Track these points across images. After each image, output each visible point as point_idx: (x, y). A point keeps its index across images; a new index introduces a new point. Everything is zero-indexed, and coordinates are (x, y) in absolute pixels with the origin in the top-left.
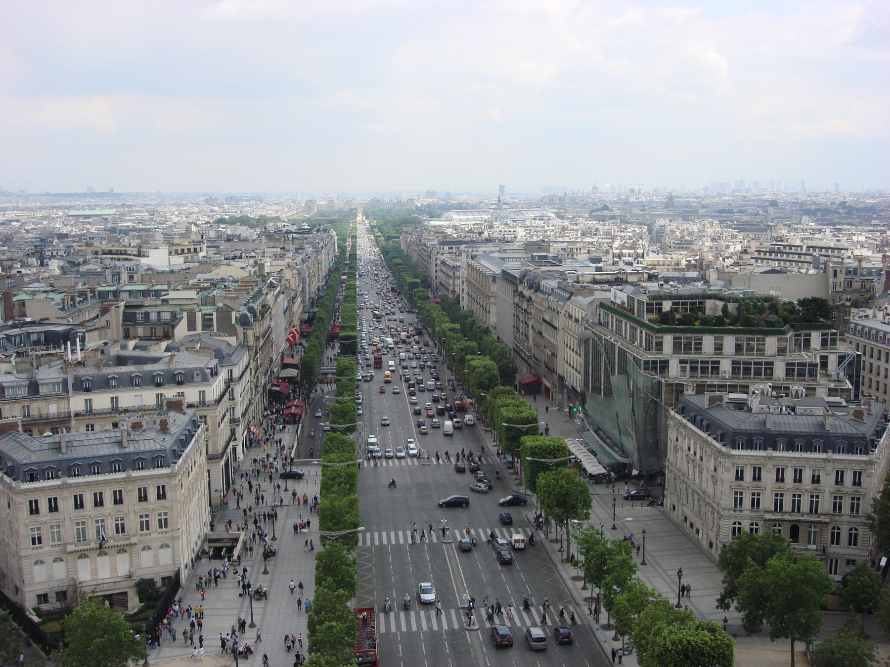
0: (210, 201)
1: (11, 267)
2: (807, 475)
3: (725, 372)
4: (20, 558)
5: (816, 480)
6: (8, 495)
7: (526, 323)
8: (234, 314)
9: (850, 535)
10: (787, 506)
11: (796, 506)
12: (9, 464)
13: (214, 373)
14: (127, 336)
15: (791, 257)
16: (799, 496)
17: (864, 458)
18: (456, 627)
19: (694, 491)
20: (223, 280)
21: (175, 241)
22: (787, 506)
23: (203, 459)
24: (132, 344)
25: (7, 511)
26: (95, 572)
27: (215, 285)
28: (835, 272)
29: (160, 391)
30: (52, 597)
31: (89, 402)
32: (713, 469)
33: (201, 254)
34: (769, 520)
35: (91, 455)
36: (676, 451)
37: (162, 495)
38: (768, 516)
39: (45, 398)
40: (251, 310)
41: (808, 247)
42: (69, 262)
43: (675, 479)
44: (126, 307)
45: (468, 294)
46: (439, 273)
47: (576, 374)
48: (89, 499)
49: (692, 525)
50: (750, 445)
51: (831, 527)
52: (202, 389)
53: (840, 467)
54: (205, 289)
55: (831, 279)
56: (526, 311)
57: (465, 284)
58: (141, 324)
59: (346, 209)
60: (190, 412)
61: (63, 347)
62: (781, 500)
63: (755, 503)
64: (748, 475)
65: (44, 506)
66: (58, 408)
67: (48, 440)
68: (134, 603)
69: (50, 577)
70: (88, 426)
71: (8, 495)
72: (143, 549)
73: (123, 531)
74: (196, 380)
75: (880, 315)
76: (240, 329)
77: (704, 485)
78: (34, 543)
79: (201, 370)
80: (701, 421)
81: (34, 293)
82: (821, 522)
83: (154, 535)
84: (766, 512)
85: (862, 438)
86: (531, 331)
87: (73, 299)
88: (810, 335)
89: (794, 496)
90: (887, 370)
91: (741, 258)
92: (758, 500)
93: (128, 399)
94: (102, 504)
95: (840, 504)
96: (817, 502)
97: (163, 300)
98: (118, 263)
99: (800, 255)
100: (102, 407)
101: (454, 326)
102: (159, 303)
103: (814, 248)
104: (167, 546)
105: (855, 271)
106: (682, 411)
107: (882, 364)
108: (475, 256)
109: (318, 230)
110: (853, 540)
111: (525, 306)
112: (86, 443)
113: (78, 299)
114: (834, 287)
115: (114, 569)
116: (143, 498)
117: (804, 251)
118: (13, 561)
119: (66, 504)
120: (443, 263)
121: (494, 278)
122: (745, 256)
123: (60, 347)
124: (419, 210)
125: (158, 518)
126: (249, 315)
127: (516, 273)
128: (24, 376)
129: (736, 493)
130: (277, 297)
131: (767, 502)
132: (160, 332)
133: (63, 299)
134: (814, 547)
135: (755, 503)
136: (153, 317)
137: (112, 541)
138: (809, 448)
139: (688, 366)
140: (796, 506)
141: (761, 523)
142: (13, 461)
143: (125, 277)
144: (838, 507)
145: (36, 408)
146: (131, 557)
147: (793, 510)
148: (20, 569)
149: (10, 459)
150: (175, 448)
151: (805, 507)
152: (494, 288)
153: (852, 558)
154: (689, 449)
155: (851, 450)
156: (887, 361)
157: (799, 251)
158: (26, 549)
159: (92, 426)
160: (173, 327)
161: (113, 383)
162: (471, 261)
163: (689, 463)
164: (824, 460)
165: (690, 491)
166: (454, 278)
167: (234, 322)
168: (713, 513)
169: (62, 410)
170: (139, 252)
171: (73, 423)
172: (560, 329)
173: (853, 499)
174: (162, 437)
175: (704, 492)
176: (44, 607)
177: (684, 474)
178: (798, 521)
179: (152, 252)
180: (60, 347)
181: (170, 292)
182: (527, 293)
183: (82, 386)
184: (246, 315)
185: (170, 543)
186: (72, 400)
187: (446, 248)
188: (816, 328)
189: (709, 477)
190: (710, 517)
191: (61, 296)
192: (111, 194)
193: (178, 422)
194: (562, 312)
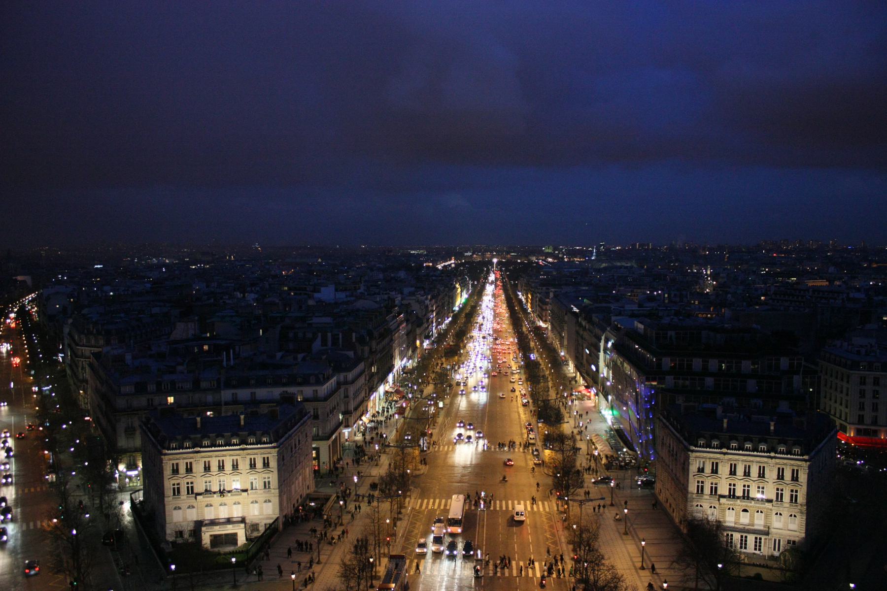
1: (222, 298)
8: (354, 334)
22: (739, 493)
29: (285, 389)
68: (242, 540)
74: (312, 380)
75: (845, 344)
90: (848, 389)
93: (262, 393)
95: (782, 494)
104: (270, 501)
107: (845, 385)
111: (581, 332)
136: (300, 335)
156: (848, 382)
161: (253, 382)
167: (354, 340)
179: (323, 289)
185: (272, 499)
186: (222, 392)
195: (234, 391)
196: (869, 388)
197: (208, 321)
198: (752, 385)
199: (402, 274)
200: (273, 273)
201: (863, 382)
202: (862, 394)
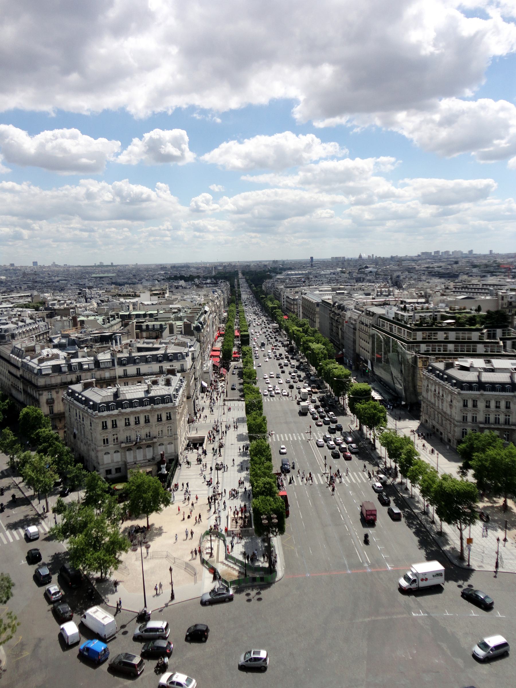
0: (163, 268)
2: (503, 404)
3: (450, 351)
4: (97, 451)
6: (90, 419)
7: (337, 327)
12: (91, 403)
13: (187, 355)
14: (137, 337)
15: (473, 291)
18: (322, 483)
19: (439, 413)
20: (183, 308)
21: (153, 289)
23: (185, 399)
24: (142, 341)
25: (90, 427)
26: (135, 457)
27: (179, 310)
29: (161, 365)
30: (113, 471)
31: (125, 371)
32: (450, 401)
33: (166, 295)
35: (133, 397)
36: (427, 391)
37: (169, 418)
38: (481, 426)
39: (103, 369)
40: (201, 323)
42: (101, 300)
43: (427, 406)
44: (137, 322)
45: (303, 313)
46: (285, 303)
47: (366, 353)
48: (132, 420)
49: (437, 430)
52: (182, 363)
54: (174, 313)
55: (500, 301)
56: (337, 321)
57: (301, 308)
58: (144, 331)
59: (233, 271)
60: (179, 375)
61: (110, 343)
63: (474, 419)
64: (470, 404)
65: (109, 424)
66: (110, 374)
67: (110, 390)
69: (112, 461)
70: (125, 383)
71: (90, 419)
72: (160, 445)
73: (149, 436)
74: (179, 358)
76: (195, 332)
77: (445, 410)
78: (104, 443)
79: (181, 353)
80: (442, 376)
81: (88, 316)
82: (510, 429)
83: (165, 438)
84: (481, 423)
86: (340, 331)
87: (108, 319)
88: (496, 331)
91: (445, 292)
93: (144, 368)
94: (139, 423)
97: (155, 319)
98: (128, 301)
100: (132, 373)
101: (299, 329)
102: (154, 320)
104: (172, 443)
108: (306, 293)
109: (221, 282)
112: (130, 391)
113: (111, 319)
114: (502, 305)
115: (145, 456)
116: (159, 419)
117: (481, 287)
118: (93, 454)
119: (121, 423)
120: (288, 297)
121: (318, 304)
122: (447, 291)
123: (108, 343)
124: (269, 271)
125: (167, 429)
126: (200, 325)
127: (330, 302)
128: (92, 358)
130: (209, 316)
132: (154, 334)
133: (103, 320)
135: (474, 419)
136: (150, 327)
137: (144, 441)
139: (430, 348)
142: (93, 402)
143: (131, 307)
145: (99, 374)
146: (153, 449)
147: (496, 423)
148: (97, 457)
149: (91, 401)
150: (175, 393)
152: (318, 309)
154: (435, 391)
157: (478, 287)
158: (101, 447)
159: (127, 383)
160: (162, 332)
161: (137, 361)
162: (304, 296)
163: (435, 398)
164: (513, 396)
165: (436, 413)
166: (294, 304)
167: (192, 329)
168: (450, 424)
169: (112, 375)
170: (135, 294)
171: (118, 381)
172: (357, 330)
174: (167, 388)
175: (445, 413)
176: (109, 476)
177: (432, 404)
180: (108, 343)
181: (159, 314)
182: (337, 311)
183: (121, 363)
184: (199, 326)
185: (173, 441)
187: (288, 289)
189: (448, 405)
190: (448, 426)
191: (102, 317)
192: (112, 265)
193: (175, 380)
195: (125, 368)
197: (78, 319)
198: (480, 349)
199: (182, 283)
200: (87, 285)
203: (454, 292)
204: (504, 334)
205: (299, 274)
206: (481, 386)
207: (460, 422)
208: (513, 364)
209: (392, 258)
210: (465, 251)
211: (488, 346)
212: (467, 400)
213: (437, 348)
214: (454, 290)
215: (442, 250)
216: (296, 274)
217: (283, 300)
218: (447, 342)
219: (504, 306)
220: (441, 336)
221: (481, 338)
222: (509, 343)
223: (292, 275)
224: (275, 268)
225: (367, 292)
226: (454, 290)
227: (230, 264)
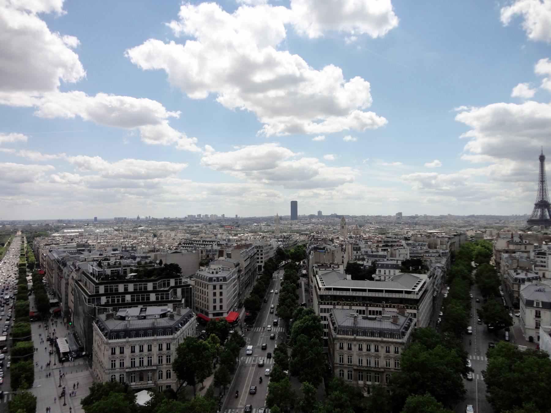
2: (146, 348)
5: (150, 350)
9: (167, 374)
10: (137, 364)
11: (141, 363)
16: (143, 358)
17: (171, 337)
22: (137, 364)
28: (202, 251)
34: (128, 372)
38: (127, 370)
41: (203, 241)
50: (118, 337)
51: (158, 371)
53: (160, 342)
62: (134, 362)
63: (122, 365)
64: (118, 351)
84: (127, 368)
85: (170, 327)
89: (140, 358)
92: (123, 363)
96: (151, 360)
99: (200, 244)
103: (205, 241)
105: (210, 251)
106: (97, 323)
110: (168, 376)
114: (202, 257)
122: (180, 246)
129: (112, 361)
131: (127, 363)
134: (150, 382)
135: (122, 365)
138: (146, 335)
140: (141, 363)
141: (125, 374)
144: (160, 361)
147: (140, 366)
151: (145, 363)
153: (169, 384)
155: (164, 334)
157: (200, 243)
173: (167, 356)
178: (142, 370)
187: (47, 247)
188: (172, 278)
194: (71, 277)
196: (218, 291)
201: (215, 288)
202: (215, 294)
203: (183, 247)
204: (176, 283)
205: (75, 232)
206: (127, 333)
207: (109, 370)
208: (162, 310)
209: (165, 218)
210: (219, 215)
211: (159, 295)
212: (115, 348)
213: (116, 299)
214: (183, 245)
215: (203, 214)
216: (72, 232)
217: (40, 257)
218: (126, 292)
219: (204, 258)
220: (121, 288)
221: (154, 287)
222: (179, 290)
223: (68, 233)
224: (58, 227)
225: (115, 248)
226: (183, 245)
227: (12, 223)
